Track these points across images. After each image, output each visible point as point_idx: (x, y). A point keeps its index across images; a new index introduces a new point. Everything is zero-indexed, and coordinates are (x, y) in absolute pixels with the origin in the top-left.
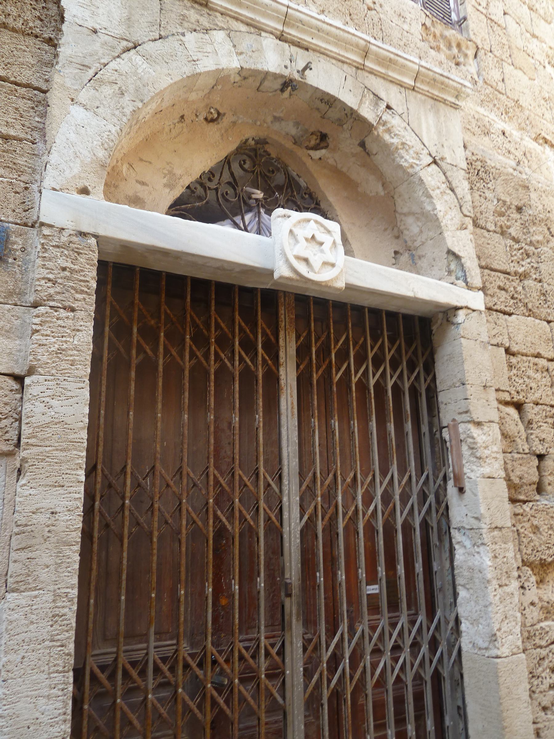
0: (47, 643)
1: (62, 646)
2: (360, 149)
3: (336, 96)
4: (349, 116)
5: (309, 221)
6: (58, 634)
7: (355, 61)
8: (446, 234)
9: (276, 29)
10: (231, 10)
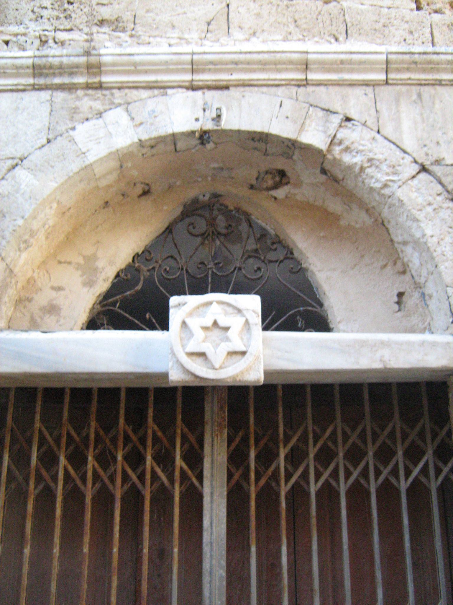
2: (323, 178)
3: (266, 130)
4: (292, 147)
5: (210, 303)
7: (293, 80)
8: (442, 268)
9: (183, 81)
10: (128, 82)
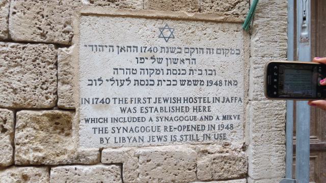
0: (273, 128)
1: (280, 131)
6: (278, 124)
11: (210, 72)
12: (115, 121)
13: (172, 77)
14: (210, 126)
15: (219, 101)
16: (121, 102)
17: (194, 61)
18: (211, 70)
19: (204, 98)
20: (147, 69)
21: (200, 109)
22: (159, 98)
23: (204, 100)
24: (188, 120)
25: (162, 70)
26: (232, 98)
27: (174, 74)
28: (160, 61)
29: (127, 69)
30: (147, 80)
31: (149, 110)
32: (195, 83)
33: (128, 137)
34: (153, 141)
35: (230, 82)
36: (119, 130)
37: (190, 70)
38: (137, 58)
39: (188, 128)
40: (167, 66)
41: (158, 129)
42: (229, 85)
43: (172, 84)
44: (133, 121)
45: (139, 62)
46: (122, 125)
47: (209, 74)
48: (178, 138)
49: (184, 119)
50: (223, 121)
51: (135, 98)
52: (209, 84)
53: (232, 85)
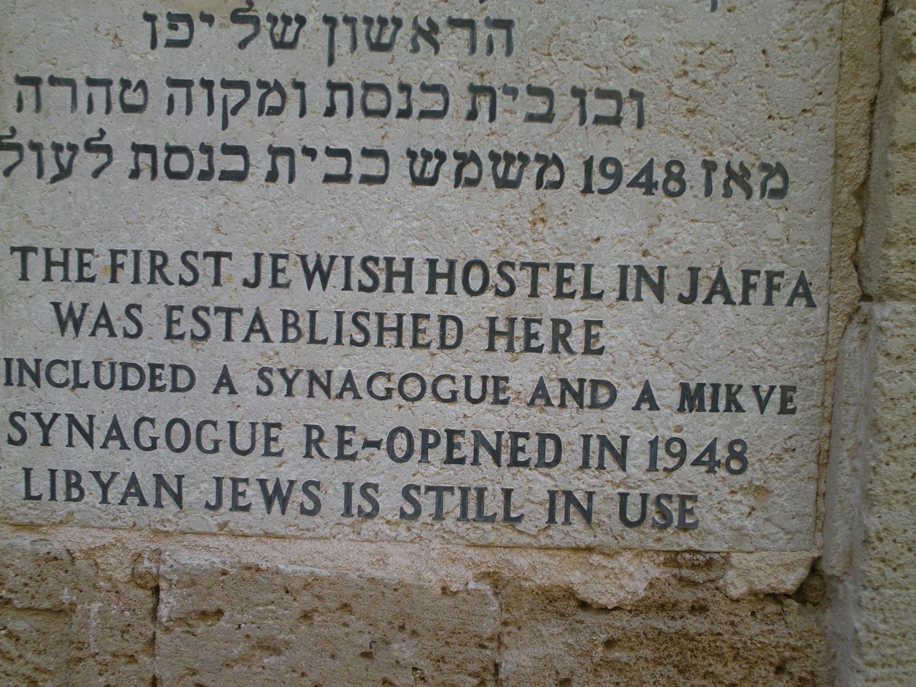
11: (607, 107)
12: (28, 379)
13: (355, 132)
14: (594, 444)
15: (659, 291)
16: (57, 272)
17: (499, 35)
18: (613, 95)
19: (561, 267)
20: (207, 84)
21: (530, 336)
22: (275, 258)
23: (561, 280)
24: (454, 399)
25: (300, 86)
26: (747, 274)
27: (368, 113)
28: (289, 37)
29: (91, 82)
30: (206, 149)
31: (217, 323)
32: (507, 169)
33: (96, 475)
34: (235, 507)
35: (738, 177)
36: (46, 428)
37: (475, 90)
38: (150, 18)
39: (452, 446)
40: (331, 61)
41: (268, 439)
42: (728, 193)
43: (357, 171)
44: (125, 387)
45: (161, 40)
46: (64, 402)
47: (598, 120)
48: (390, 501)
49: (430, 388)
50: (680, 419)
51: (137, 253)
52: (600, 182)
53: (749, 194)
